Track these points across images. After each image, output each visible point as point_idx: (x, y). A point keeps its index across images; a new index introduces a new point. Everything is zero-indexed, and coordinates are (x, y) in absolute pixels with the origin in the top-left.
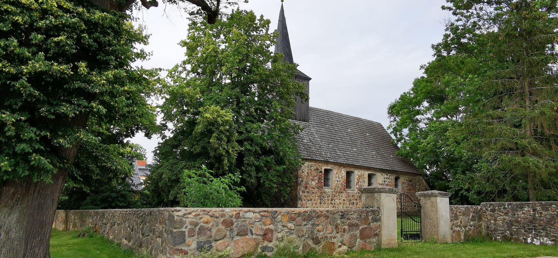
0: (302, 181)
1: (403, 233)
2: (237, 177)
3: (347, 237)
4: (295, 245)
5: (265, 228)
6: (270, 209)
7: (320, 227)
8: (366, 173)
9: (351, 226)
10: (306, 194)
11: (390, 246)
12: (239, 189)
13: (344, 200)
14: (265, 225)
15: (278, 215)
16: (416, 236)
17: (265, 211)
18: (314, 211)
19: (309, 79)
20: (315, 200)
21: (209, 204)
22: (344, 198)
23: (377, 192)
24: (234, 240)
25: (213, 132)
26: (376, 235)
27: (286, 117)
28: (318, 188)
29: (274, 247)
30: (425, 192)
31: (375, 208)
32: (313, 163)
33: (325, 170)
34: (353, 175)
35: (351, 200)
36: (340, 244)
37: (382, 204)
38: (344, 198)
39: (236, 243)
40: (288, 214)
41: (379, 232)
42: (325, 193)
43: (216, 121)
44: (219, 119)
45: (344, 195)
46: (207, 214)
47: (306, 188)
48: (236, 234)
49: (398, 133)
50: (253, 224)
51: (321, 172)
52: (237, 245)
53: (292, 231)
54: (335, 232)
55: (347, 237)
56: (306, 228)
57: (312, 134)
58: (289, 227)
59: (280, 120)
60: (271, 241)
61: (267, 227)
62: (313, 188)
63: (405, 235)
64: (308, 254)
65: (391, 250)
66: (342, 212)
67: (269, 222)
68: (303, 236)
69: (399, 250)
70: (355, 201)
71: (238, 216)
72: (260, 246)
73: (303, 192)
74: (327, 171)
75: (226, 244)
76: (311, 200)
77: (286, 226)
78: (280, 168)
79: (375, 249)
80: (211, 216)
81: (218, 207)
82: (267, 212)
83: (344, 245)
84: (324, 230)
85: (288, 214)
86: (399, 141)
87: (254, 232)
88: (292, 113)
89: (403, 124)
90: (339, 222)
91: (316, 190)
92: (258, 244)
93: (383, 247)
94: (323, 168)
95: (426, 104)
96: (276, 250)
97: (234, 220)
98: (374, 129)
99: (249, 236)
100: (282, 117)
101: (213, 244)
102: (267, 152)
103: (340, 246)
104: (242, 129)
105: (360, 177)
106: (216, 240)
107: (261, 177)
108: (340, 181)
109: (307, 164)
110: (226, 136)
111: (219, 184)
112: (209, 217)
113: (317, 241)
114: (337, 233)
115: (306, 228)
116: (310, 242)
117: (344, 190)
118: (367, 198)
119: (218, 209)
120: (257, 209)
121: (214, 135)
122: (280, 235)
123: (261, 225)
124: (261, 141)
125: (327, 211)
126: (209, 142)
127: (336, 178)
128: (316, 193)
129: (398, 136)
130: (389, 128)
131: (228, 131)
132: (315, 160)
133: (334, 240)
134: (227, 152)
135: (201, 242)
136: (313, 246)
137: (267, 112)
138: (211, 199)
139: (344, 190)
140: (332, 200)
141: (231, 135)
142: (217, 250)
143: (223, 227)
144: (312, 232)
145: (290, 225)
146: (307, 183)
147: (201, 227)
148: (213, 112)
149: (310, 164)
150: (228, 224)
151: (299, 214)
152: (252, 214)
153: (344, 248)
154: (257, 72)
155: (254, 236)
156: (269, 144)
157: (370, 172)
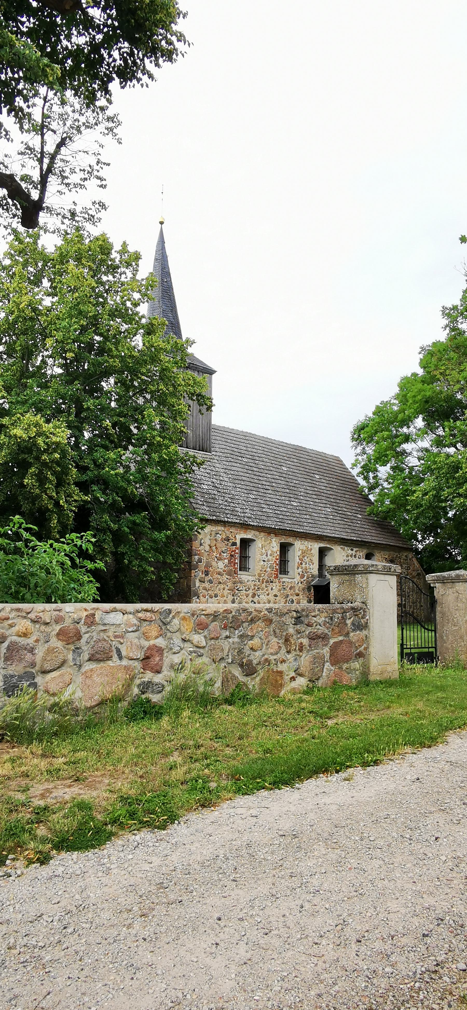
0: (200, 561)
1: (406, 651)
2: (86, 540)
3: (305, 660)
4: (207, 678)
5: (146, 644)
6: (157, 606)
7: (256, 642)
8: (316, 546)
9: (314, 638)
10: (207, 585)
11: (386, 676)
12: (90, 565)
13: (276, 596)
14: (147, 638)
15: (174, 617)
16: (428, 657)
17: (146, 611)
18: (245, 610)
19: (211, 372)
20: (223, 596)
21: (28, 596)
22: (275, 591)
23: (361, 572)
24: (83, 670)
25: (30, 465)
26: (360, 655)
27: (170, 439)
28: (229, 574)
29: (165, 683)
30: (445, 574)
31: (357, 604)
33: (243, 541)
34: (291, 549)
35: (287, 596)
36: (293, 674)
37: (370, 595)
38: (275, 591)
39: (87, 676)
40: (193, 615)
41: (366, 649)
42: (241, 582)
43: (35, 444)
44: (40, 441)
45: (276, 587)
46: (25, 617)
48: (86, 657)
49: (371, 475)
50: (123, 637)
51: (234, 544)
52: (88, 682)
53: (202, 651)
54: (283, 650)
55: (305, 660)
56: (228, 644)
58: (195, 642)
59: (160, 445)
60: (159, 672)
61: (152, 642)
62: (219, 574)
63: (407, 655)
64: (232, 695)
65: (389, 683)
66: (297, 612)
67: (154, 633)
68: (222, 659)
69: (403, 682)
70: (295, 598)
71: (91, 620)
72: (137, 682)
73: (202, 581)
74: (246, 543)
75: (67, 678)
76: (216, 596)
77: (189, 641)
78: (161, 536)
79: (359, 683)
80: (33, 621)
81: (49, 601)
82: (151, 611)
83: (301, 675)
84: (264, 647)
85: (193, 615)
86: (372, 488)
87: (124, 653)
88: (182, 432)
89: (381, 459)
90: (291, 631)
91: (225, 577)
92: (132, 679)
93: (372, 678)
94: (239, 537)
95: (419, 422)
96: (168, 688)
97: (83, 629)
98: (329, 466)
99: (115, 662)
100: (164, 438)
101: (39, 680)
102: (135, 505)
103: (293, 679)
104: (87, 461)
105: (304, 554)
106: (45, 672)
107: (123, 554)
108: (268, 561)
109: (209, 528)
110: (54, 473)
111: (49, 555)
112: (29, 623)
113: (249, 670)
114: (289, 652)
115: (228, 644)
116: (237, 672)
117: (276, 577)
118: (341, 584)
119: (48, 606)
120: (130, 607)
121: (33, 470)
122: (177, 659)
123: (139, 639)
124: (124, 484)
125: (270, 610)
126: (22, 486)
127: (262, 555)
128: (225, 583)
129: (372, 481)
130: (354, 465)
131: (58, 463)
132: (224, 522)
133: (282, 667)
134: (57, 504)
135: (12, 676)
136: (242, 679)
137: (135, 431)
138: (32, 585)
139: (276, 577)
140: (254, 595)
141: (65, 471)
142: (47, 691)
143: (59, 644)
144: (240, 652)
145: (198, 639)
146: (208, 565)
147: (12, 644)
148: (29, 426)
149: (215, 528)
150: (71, 637)
151: (215, 616)
152: (119, 617)
153: (302, 682)
154: (115, 353)
155: (125, 662)
156: (139, 490)
157: (322, 545)
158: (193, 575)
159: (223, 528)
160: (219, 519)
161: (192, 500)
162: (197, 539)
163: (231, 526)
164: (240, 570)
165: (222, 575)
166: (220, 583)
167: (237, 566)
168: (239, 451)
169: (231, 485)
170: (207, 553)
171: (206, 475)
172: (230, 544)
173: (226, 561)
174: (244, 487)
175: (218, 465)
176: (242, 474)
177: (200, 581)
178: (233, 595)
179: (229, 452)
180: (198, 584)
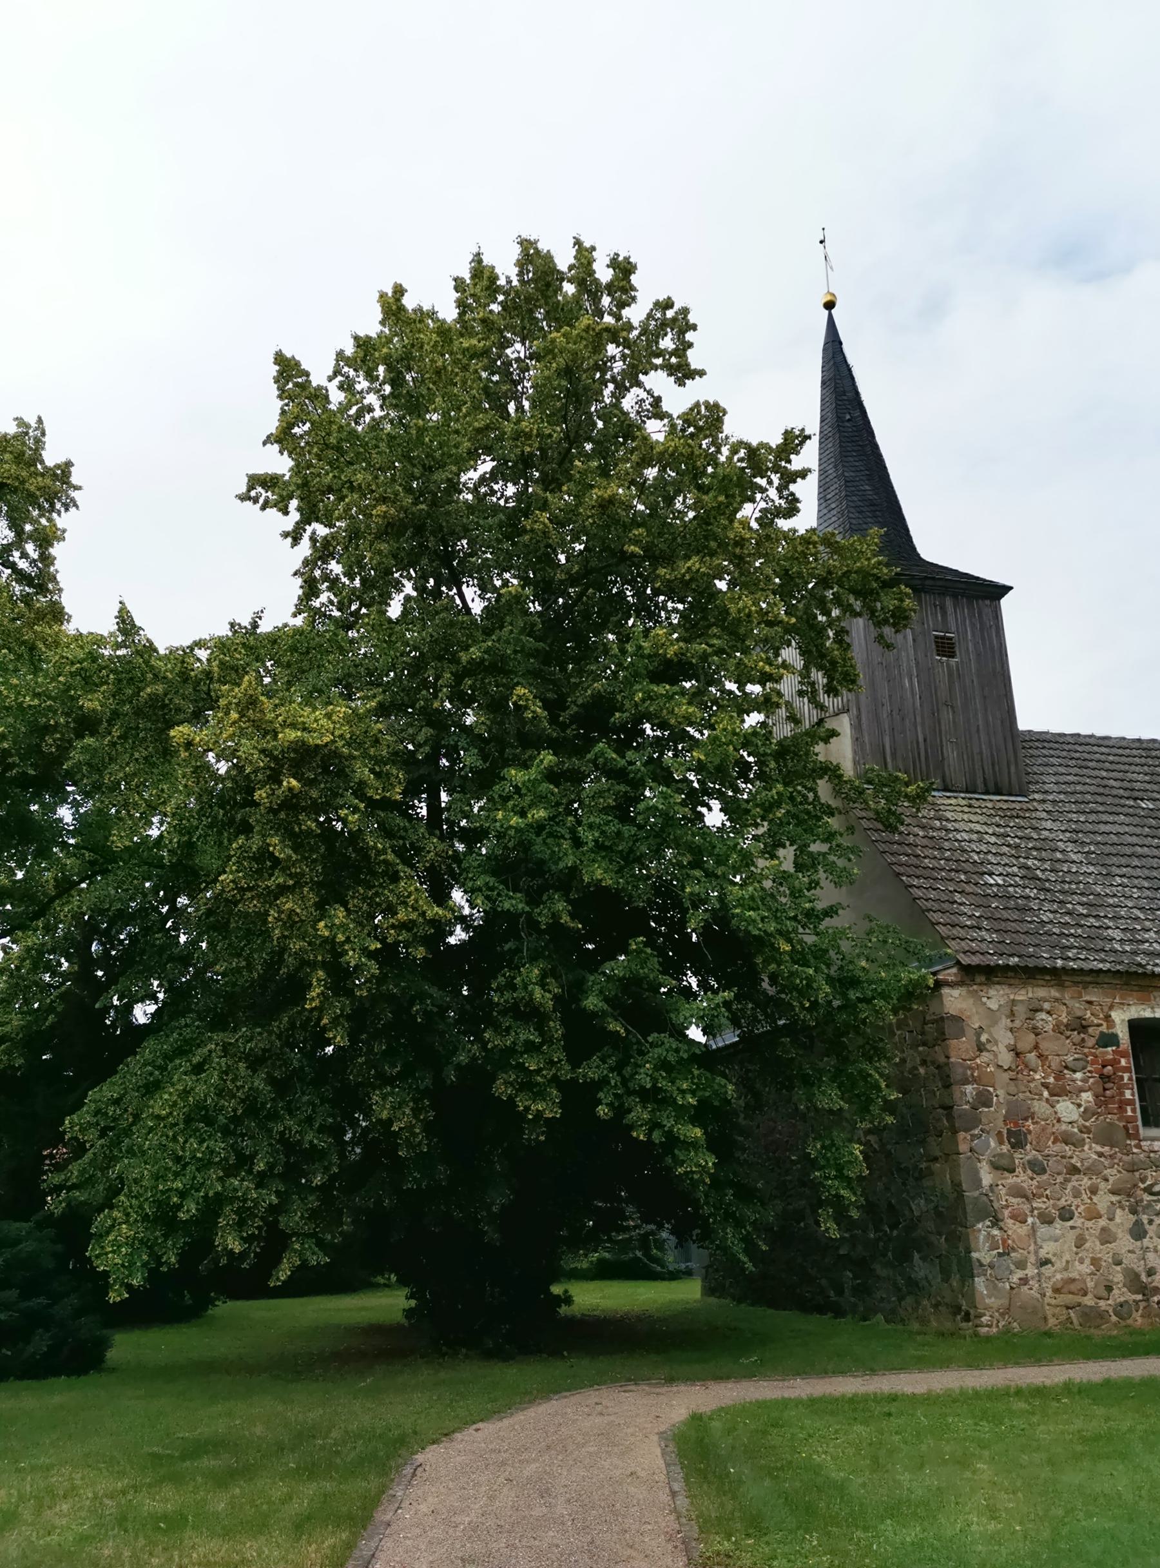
0: (984, 1100)
10: (1022, 1178)
28: (1105, 1137)
32: (1041, 992)
47: (1017, 1140)
51: (1109, 1040)
57: (1045, 846)
62: (1067, 1139)
73: (1003, 1167)
76: (1066, 1215)
91: (1091, 1151)
94: (1120, 1018)
109: (996, 997)
128: (1091, 1171)
132: (1054, 972)
146: (1018, 1115)
149: (1022, 995)
158: (963, 1147)
159: (1054, 993)
160: (1031, 963)
161: (936, 917)
162: (961, 1033)
163: (1086, 985)
164: (1146, 1123)
165: (1078, 1144)
166: (1074, 1170)
167: (1133, 1112)
168: (1126, 784)
169: (1091, 869)
170: (1006, 1076)
171: (1005, 849)
172: (1091, 1042)
173: (1087, 1097)
174: (1138, 872)
175: (1049, 824)
176: (1134, 840)
177: (996, 1167)
178: (1134, 1211)
179: (1092, 789)
180: (987, 1178)
